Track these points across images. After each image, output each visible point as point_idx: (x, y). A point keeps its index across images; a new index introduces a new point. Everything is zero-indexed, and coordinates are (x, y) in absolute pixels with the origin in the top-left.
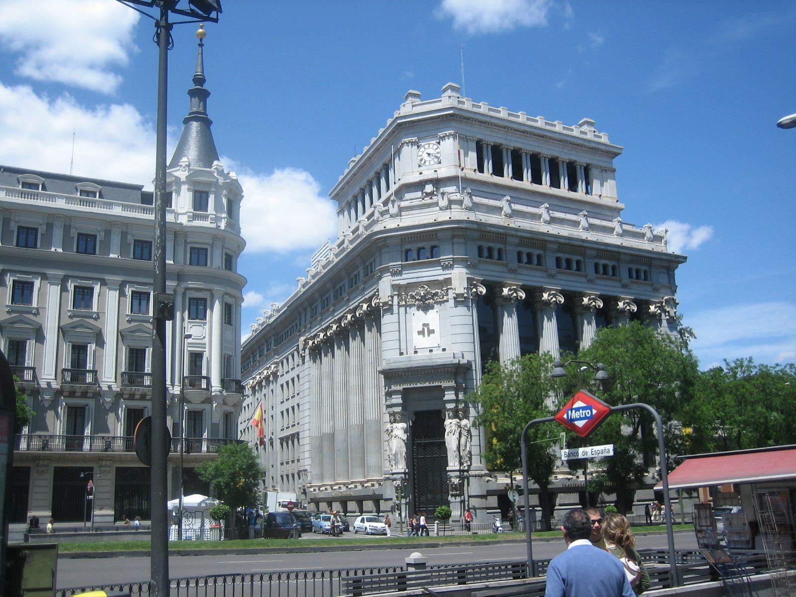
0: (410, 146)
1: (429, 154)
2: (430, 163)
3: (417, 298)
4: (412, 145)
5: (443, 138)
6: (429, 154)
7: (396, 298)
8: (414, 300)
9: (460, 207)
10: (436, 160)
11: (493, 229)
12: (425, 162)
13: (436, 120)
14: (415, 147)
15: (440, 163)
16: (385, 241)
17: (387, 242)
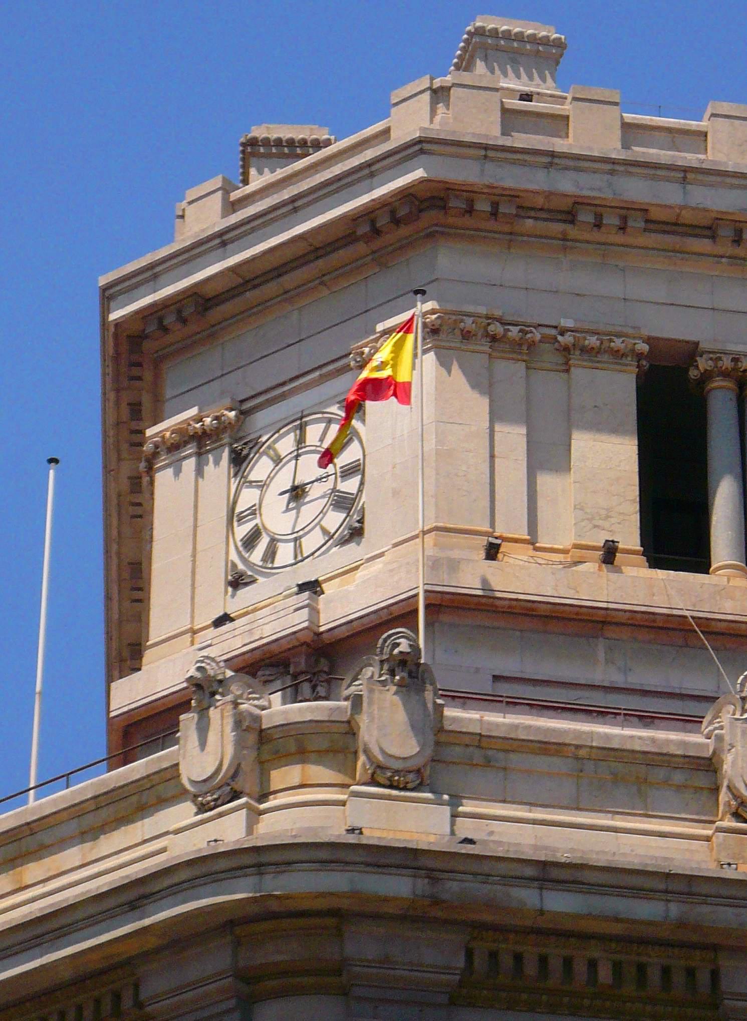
0: (190, 465)
2: (298, 549)
4: (200, 454)
9: (339, 778)
11: (559, 903)
12: (271, 554)
13: (343, 254)
14: (218, 470)
15: (356, 533)
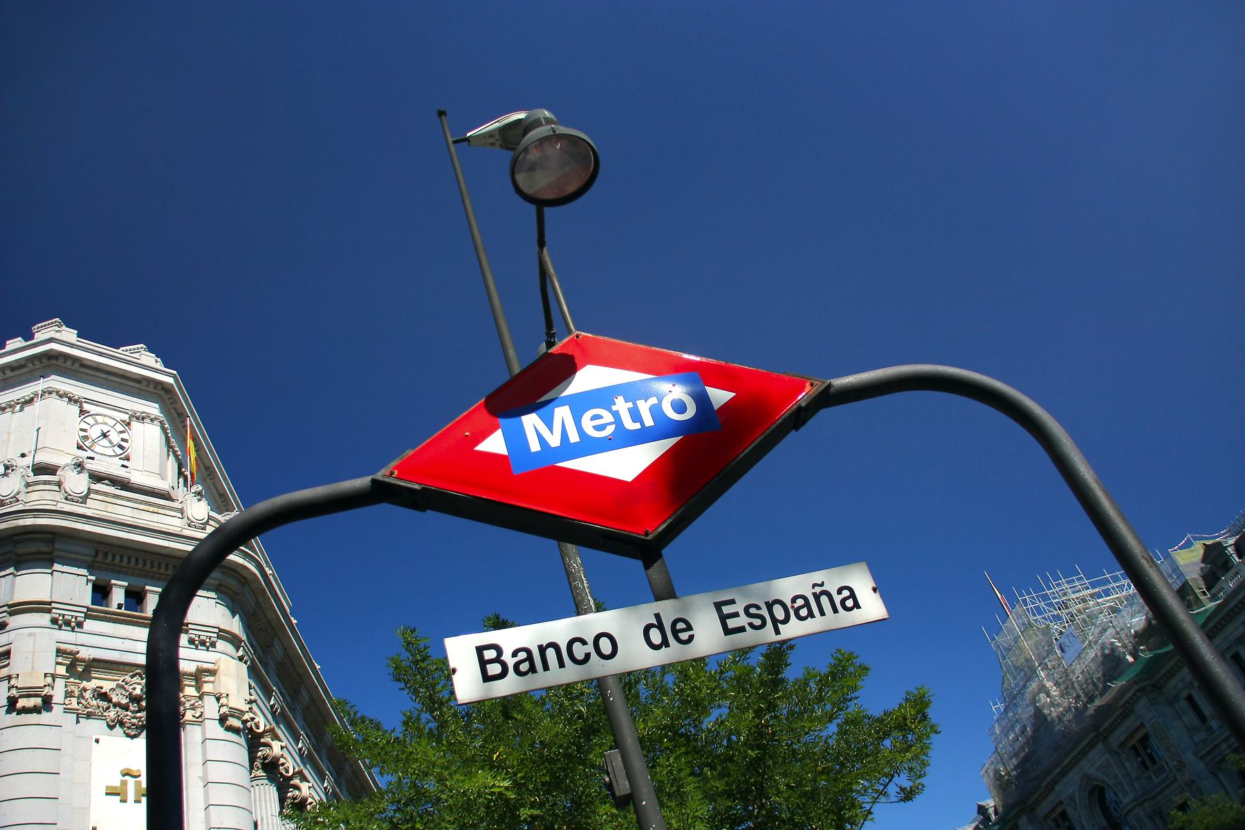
1: (105, 435)
3: (115, 700)
5: (141, 418)
6: (105, 435)
7: (60, 683)
8: (105, 704)
10: (119, 451)
16: (52, 541)
17: (57, 545)
